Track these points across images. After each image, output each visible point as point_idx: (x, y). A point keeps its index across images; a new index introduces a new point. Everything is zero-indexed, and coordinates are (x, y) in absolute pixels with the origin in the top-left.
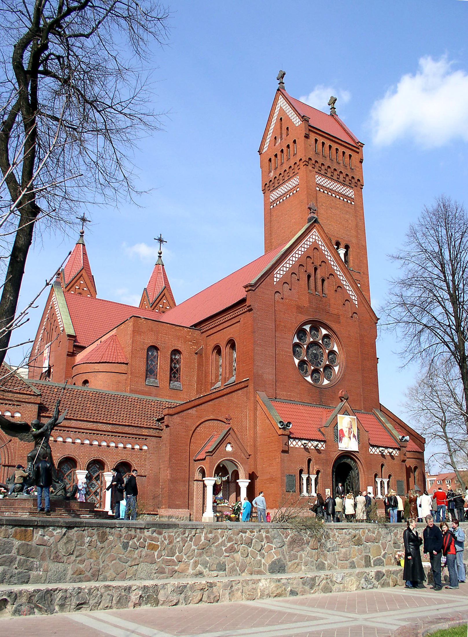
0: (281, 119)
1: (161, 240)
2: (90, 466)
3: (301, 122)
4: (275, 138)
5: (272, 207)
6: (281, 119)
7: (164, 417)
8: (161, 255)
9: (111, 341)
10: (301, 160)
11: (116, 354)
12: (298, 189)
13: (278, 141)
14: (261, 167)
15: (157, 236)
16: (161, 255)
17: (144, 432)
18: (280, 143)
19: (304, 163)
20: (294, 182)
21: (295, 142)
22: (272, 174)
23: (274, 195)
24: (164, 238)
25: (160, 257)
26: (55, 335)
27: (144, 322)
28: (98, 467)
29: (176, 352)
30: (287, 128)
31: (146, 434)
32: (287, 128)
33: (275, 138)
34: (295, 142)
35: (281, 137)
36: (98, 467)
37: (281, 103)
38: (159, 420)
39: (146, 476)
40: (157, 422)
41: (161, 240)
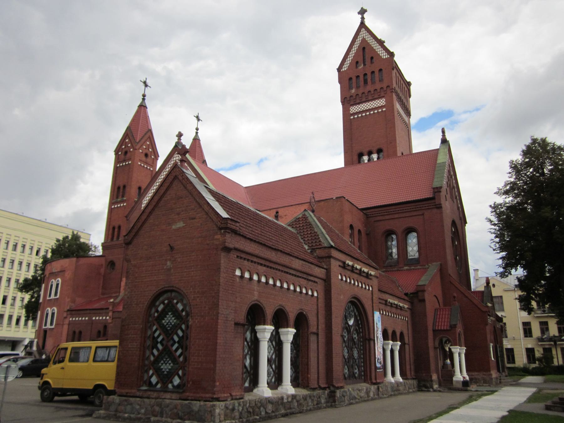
0: (364, 48)
1: (197, 117)
3: (389, 56)
4: (357, 63)
5: (352, 117)
6: (364, 48)
8: (198, 131)
10: (388, 86)
12: (384, 109)
13: (361, 65)
14: (340, 82)
16: (198, 131)
18: (363, 68)
19: (391, 91)
20: (381, 102)
21: (380, 70)
22: (353, 91)
23: (354, 109)
25: (197, 133)
30: (372, 58)
32: (372, 58)
33: (357, 63)
34: (380, 70)
35: (365, 65)
37: (364, 35)
41: (197, 117)
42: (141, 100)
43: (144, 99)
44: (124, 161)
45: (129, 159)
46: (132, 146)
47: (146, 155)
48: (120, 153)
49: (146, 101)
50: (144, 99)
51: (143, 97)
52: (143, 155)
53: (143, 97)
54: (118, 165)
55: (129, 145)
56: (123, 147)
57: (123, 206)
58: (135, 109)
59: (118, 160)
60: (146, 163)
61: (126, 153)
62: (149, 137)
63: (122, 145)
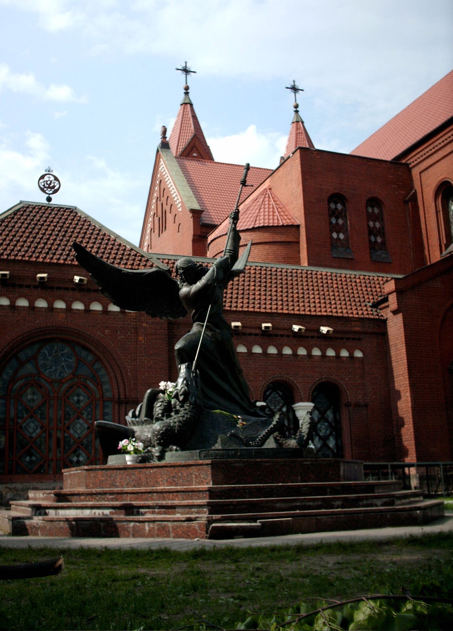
1: (295, 89)
2: (268, 393)
7: (387, 297)
8: (298, 109)
9: (265, 197)
11: (277, 213)
15: (290, 84)
16: (298, 109)
17: (355, 327)
24: (299, 85)
25: (297, 112)
26: (170, 217)
27: (318, 157)
28: (281, 393)
29: (373, 202)
31: (357, 329)
36: (281, 393)
38: (375, 305)
39: (366, 405)
40: (374, 310)
41: (295, 89)
43: (187, 93)
49: (191, 95)
50: (187, 93)
51: (185, 91)
53: (185, 91)
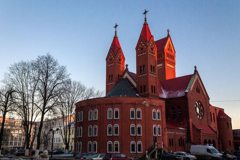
42: (144, 21)
44: (142, 53)
45: (145, 52)
46: (145, 45)
47: (152, 49)
48: (139, 49)
52: (151, 49)
54: (139, 56)
55: (143, 45)
56: (140, 46)
57: (145, 75)
58: (142, 26)
59: (138, 53)
60: (152, 53)
61: (142, 49)
62: (152, 40)
63: (139, 45)
